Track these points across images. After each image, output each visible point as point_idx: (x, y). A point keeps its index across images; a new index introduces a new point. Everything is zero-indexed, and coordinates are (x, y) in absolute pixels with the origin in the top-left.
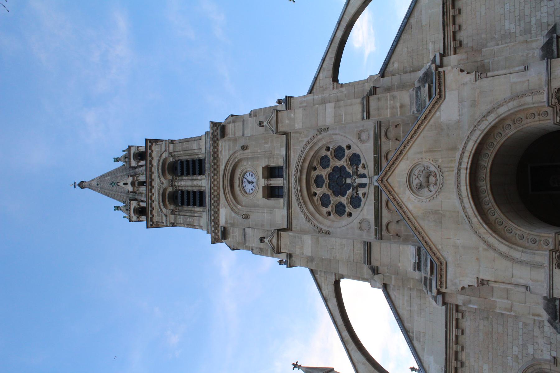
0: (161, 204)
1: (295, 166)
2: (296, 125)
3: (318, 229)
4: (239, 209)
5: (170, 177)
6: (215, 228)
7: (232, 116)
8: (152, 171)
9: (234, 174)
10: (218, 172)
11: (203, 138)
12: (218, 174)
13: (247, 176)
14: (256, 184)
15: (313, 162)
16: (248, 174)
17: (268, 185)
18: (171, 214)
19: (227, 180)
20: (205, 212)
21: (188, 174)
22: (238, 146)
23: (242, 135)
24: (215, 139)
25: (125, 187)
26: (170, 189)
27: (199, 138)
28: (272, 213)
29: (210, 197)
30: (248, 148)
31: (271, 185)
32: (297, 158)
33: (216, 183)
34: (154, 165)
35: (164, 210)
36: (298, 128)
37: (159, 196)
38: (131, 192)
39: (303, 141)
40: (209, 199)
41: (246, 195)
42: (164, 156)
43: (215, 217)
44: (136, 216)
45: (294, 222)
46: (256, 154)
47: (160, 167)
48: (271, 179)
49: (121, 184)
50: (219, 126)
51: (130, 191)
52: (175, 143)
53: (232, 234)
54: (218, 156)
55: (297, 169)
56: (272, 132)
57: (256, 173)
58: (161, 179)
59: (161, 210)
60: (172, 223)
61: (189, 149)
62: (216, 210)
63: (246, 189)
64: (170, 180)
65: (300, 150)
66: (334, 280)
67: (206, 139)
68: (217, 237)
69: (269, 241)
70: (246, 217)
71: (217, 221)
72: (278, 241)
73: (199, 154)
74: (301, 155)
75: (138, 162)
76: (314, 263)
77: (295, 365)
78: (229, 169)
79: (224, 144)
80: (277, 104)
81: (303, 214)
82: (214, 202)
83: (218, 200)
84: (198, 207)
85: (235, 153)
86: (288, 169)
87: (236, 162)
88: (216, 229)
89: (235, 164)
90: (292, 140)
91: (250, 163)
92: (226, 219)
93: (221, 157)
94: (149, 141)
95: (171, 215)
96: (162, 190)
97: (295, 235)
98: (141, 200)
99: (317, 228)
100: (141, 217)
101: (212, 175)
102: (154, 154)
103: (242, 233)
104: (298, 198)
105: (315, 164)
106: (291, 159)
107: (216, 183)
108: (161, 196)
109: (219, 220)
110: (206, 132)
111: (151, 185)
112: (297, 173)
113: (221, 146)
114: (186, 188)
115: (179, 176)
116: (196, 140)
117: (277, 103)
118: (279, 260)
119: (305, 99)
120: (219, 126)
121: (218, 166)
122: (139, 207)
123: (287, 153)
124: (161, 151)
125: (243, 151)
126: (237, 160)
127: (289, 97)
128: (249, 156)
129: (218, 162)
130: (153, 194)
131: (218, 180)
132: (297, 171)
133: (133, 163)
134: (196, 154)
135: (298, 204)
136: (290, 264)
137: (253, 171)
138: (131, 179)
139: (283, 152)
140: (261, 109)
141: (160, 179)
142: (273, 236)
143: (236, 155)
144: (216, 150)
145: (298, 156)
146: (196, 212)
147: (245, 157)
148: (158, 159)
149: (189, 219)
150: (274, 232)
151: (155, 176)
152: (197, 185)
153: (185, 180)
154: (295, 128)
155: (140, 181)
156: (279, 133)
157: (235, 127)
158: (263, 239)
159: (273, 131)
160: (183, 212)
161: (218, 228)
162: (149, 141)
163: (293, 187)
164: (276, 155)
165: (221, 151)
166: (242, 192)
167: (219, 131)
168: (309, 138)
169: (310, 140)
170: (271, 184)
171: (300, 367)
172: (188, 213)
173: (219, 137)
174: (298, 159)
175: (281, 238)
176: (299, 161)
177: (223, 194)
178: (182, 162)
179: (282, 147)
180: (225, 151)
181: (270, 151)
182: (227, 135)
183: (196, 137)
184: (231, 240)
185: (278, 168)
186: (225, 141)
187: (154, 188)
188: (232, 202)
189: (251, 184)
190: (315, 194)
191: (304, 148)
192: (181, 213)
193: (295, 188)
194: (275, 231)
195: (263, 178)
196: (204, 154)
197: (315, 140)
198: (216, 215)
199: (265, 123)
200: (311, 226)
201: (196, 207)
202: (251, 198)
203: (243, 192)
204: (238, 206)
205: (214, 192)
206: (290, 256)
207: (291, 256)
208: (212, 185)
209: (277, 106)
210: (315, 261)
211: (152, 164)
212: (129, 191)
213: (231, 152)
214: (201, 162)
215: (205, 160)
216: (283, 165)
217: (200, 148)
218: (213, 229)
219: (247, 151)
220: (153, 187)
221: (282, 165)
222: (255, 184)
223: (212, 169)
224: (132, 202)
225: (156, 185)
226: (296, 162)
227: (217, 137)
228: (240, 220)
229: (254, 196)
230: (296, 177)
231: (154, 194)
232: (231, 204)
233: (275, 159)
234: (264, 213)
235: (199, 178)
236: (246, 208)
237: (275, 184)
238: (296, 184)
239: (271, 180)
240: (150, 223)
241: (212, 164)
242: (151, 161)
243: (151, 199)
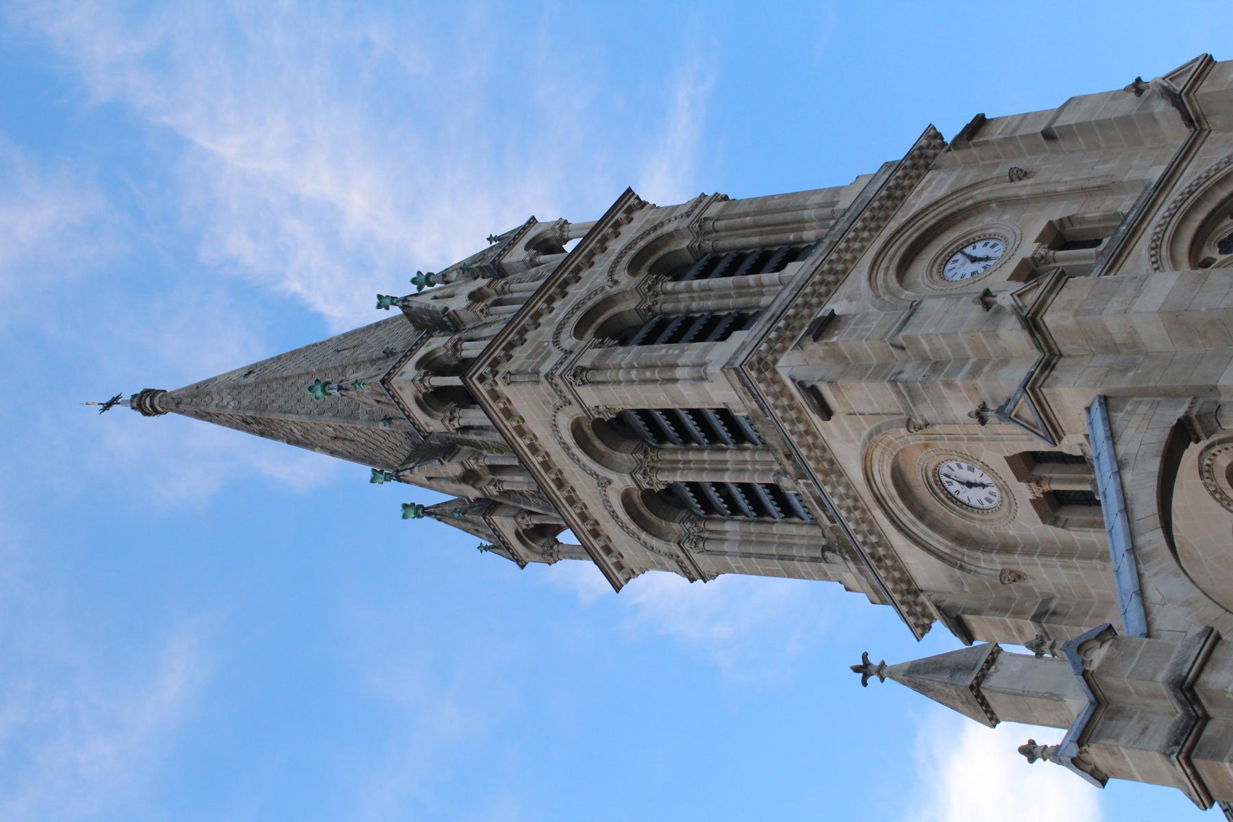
6: (779, 337)
9: (930, 241)
10: (878, 228)
34: (610, 248)
47: (633, 252)
54: (903, 197)
66: (1181, 412)
72: (1050, 292)
75: (537, 255)
77: (864, 670)
86: (1160, 192)
106: (1179, 179)
108: (579, 314)
112: (1184, 201)
121: (887, 218)
123: (1176, 163)
126: (968, 203)
129: (894, 209)
130: (553, 309)
131: (859, 255)
143: (975, 193)
161: (796, 333)
163: (1153, 224)
171: (882, 671)
187: (568, 297)
207: (1050, 368)
210: (1138, 369)
220: (564, 295)
223: (867, 214)
238: (1168, 220)
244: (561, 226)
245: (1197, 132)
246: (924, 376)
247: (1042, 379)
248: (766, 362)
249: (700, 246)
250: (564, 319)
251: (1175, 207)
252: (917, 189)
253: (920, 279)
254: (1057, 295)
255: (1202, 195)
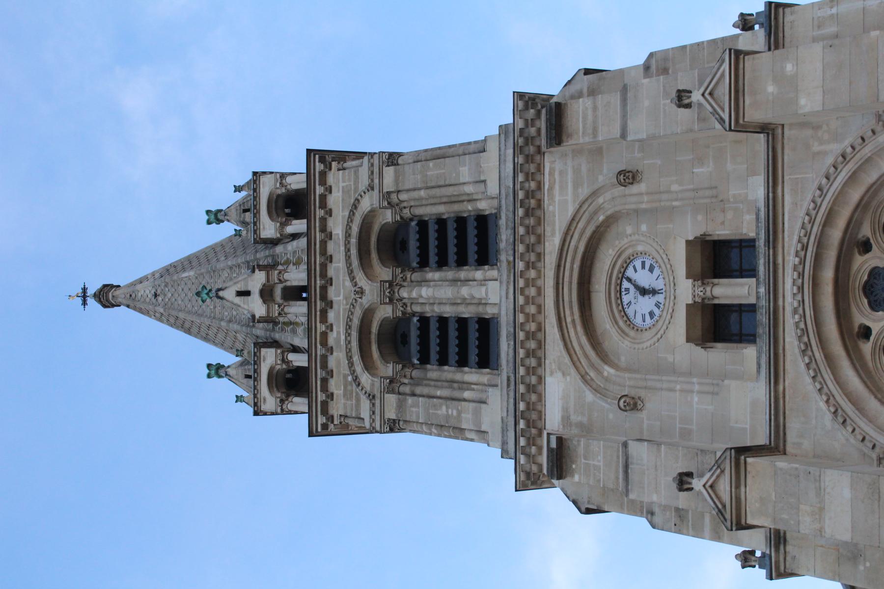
0: (356, 358)
1: (796, 238)
2: (803, 101)
3: (877, 450)
4: (607, 379)
5: (385, 273)
7: (588, 72)
8: (329, 254)
10: (540, 256)
11: (493, 148)
12: (539, 265)
13: (636, 271)
14: (665, 298)
15: (859, 224)
16: (638, 263)
17: (703, 299)
18: (388, 392)
19: (570, 283)
20: (496, 386)
21: (442, 263)
22: (605, 171)
23: (618, 136)
24: (532, 149)
25: (242, 305)
26: (386, 312)
27: (477, 145)
28: (717, 394)
29: (512, 338)
30: (638, 179)
31: (716, 302)
32: (804, 211)
33: (532, 291)
35: (365, 379)
36: (807, 110)
37: (348, 335)
38: (262, 320)
39: (825, 153)
40: (509, 344)
41: (632, 333)
42: (366, 205)
43: (528, 404)
44: (276, 398)
45: (794, 427)
46: (665, 196)
47: (354, 241)
48: (716, 281)
49: (229, 294)
50: (542, 107)
51: (257, 317)
52: (400, 161)
53: (583, 461)
55: (805, 248)
56: (718, 126)
57: (666, 261)
58: (357, 279)
59: (356, 379)
60: (389, 420)
61: (447, 183)
62: (534, 380)
63: (630, 312)
64: (386, 282)
65: (816, 185)
67: (503, 148)
68: (535, 468)
69: (707, 486)
70: (632, 404)
71: (534, 416)
72: (738, 487)
73: (480, 197)
74: (819, 200)
75: (283, 225)
76: (861, 568)
78: (576, 248)
79: (558, 166)
80: (738, 31)
81: (825, 398)
82: (528, 355)
83: (540, 348)
84: (473, 370)
85: (594, 194)
86: (774, 248)
87: (598, 223)
88: (531, 442)
89: (594, 232)
90: (786, 151)
91: (644, 228)
92: (565, 410)
93: (551, 208)
94: (317, 156)
95: (386, 396)
96: (358, 313)
97: (796, 469)
98: (292, 345)
99: (874, 447)
100: (290, 399)
101: (520, 265)
102: (335, 200)
103: (618, 457)
104: (808, 345)
105: (866, 231)
106: (783, 215)
107: (532, 291)
109: (540, 412)
110: (500, 126)
111: (324, 297)
112: (803, 262)
113: (551, 174)
114: (437, 309)
115: (414, 270)
116: (469, 154)
117: (738, 27)
118: (739, 550)
119: (834, 11)
120: (542, 107)
121: (540, 239)
122: (284, 366)
123: (771, 195)
124: (355, 191)
125: (623, 188)
126: (601, 218)
127: (778, 5)
128: (644, 206)
129: (539, 224)
130: (332, 325)
131: (539, 283)
132: (803, 253)
133: (269, 229)
134: (470, 198)
135: (808, 366)
136: (778, 568)
137: (655, 254)
138: (260, 278)
139: (758, 190)
140: (684, 48)
141: (352, 279)
142: (722, 471)
143: (601, 200)
144: (533, 185)
145: (806, 204)
146: (465, 385)
147: (627, 207)
148: (347, 214)
149: (444, 408)
150: (725, 458)
151: (337, 268)
152: (473, 297)
153: (432, 283)
154: (800, 112)
155: (288, 284)
156: (743, 126)
157: (595, 109)
158: (689, 480)
159: (724, 122)
160: (426, 385)
162: (317, 156)
163: (789, 310)
164: (732, 200)
165: (551, 188)
166: (617, 323)
167: (542, 124)
168: (847, 142)
169: (849, 150)
170: (714, 298)
172: (441, 387)
173: (544, 142)
174: (807, 214)
175: (748, 476)
176: (812, 222)
177: (556, 330)
178: (423, 225)
179: (754, 174)
180: (563, 188)
181: (711, 188)
182: (570, 136)
183: (469, 143)
184: (580, 479)
185: (737, 245)
186: (564, 155)
187: (335, 306)
188: (586, 356)
189: (647, 297)
190: (866, 333)
191: (828, 178)
192: (418, 390)
193: (795, 311)
194: (728, 453)
195: (687, 278)
196: (493, 198)
197: (867, 151)
198: (534, 397)
199: (696, 97)
200: (852, 440)
201: (466, 369)
202: (648, 344)
203: (621, 323)
204: (606, 368)
205: (527, 321)
206: (778, 539)
207: (782, 541)
208: (521, 300)
209: (736, 37)
211: (329, 230)
212: (253, 316)
213: (584, 192)
214: (484, 223)
215: (496, 216)
216: (758, 234)
217: (482, 178)
218: (522, 442)
219: (635, 189)
220: (330, 304)
221: (752, 235)
222: (660, 298)
223: (521, 248)
224: (264, 351)
225: (341, 298)
226: (799, 224)
227: (538, 143)
228: (611, 416)
229: (659, 336)
230: (801, 275)
231: (335, 328)
232: (583, 360)
233: (730, 215)
234: (692, 392)
235: (479, 274)
236: (630, 375)
237: (727, 297)
238: (799, 297)
239: (714, 285)
240: (321, 420)
241: (521, 230)
242: (323, 221)
243: (324, 343)
244: (280, 184)
245: (770, 137)
246: (675, 525)
247: (782, 559)
248: (534, 474)
249: (401, 218)
250: (346, 337)
251: (799, 288)
252: (546, 187)
253: (608, 327)
254: (746, 487)
255: (818, 247)
